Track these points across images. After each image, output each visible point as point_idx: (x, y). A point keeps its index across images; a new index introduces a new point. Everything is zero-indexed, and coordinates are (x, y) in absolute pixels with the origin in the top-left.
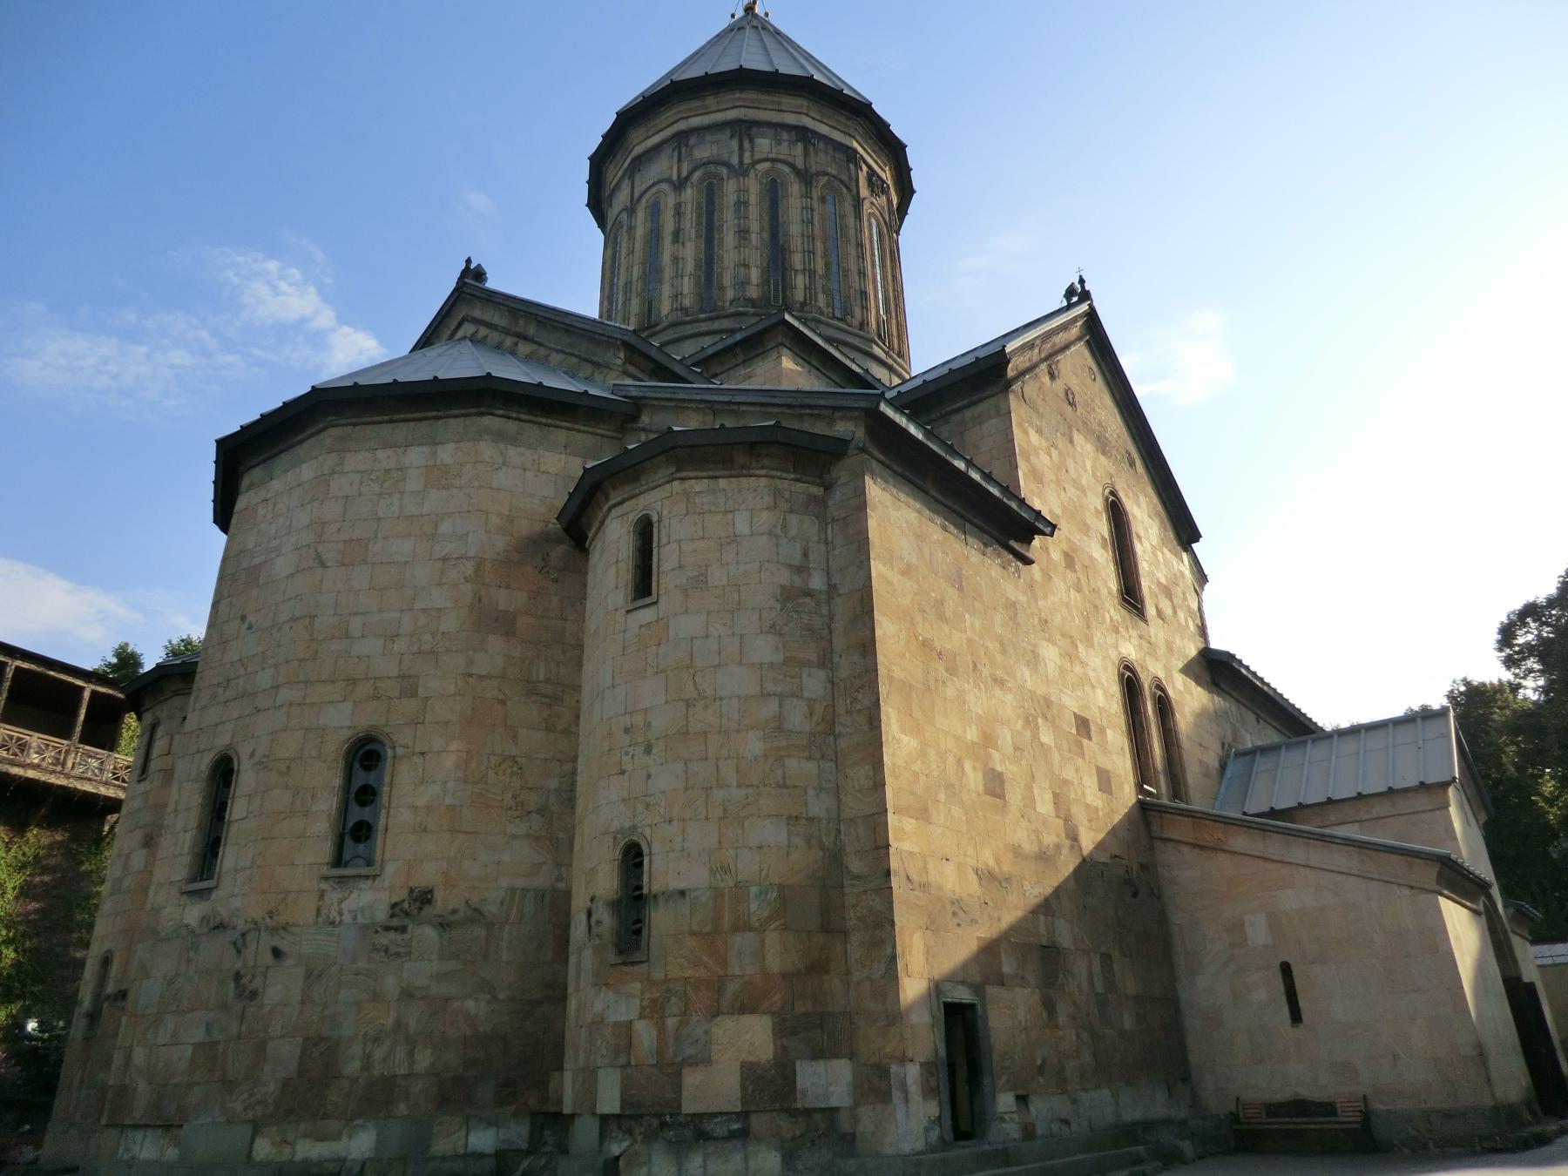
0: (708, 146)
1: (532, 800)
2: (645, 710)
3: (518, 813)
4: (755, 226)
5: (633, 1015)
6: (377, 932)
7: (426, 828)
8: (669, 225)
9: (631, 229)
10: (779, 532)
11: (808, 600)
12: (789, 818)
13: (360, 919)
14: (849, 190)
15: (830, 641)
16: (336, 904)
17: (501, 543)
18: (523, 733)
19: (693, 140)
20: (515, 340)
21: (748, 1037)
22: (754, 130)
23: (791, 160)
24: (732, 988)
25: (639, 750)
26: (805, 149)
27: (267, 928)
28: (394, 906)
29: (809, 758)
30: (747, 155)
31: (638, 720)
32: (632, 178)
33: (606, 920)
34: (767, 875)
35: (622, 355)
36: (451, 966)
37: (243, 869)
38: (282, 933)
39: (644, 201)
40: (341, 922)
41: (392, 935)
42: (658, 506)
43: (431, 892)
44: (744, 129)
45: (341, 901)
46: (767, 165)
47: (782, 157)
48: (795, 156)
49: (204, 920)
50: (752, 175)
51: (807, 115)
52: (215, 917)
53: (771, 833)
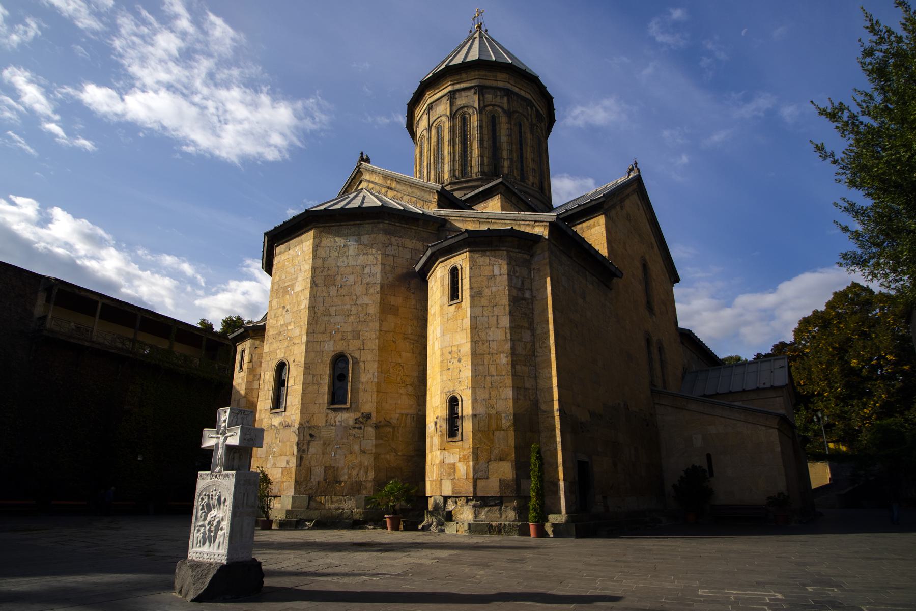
0: (463, 98)
1: (408, 380)
2: (458, 345)
3: (403, 385)
4: (486, 137)
5: (457, 459)
6: (350, 429)
7: (367, 390)
10: (512, 274)
11: (524, 302)
12: (517, 388)
13: (343, 424)
14: (528, 120)
15: (533, 319)
16: (333, 419)
17: (391, 277)
18: (404, 354)
20: (386, 190)
21: (502, 470)
22: (484, 90)
23: (501, 105)
24: (496, 451)
25: (456, 361)
26: (508, 100)
27: (307, 427)
28: (356, 419)
29: (525, 365)
30: (481, 103)
31: (455, 349)
32: (429, 114)
33: (444, 426)
34: (509, 410)
35: (436, 197)
36: (381, 442)
37: (294, 405)
38: (313, 429)
40: (335, 425)
41: (356, 430)
42: (461, 263)
43: (371, 414)
45: (335, 418)
46: (491, 108)
47: (497, 104)
48: (503, 103)
49: (281, 424)
50: (484, 113)
51: (508, 82)
52: (285, 422)
53: (509, 393)
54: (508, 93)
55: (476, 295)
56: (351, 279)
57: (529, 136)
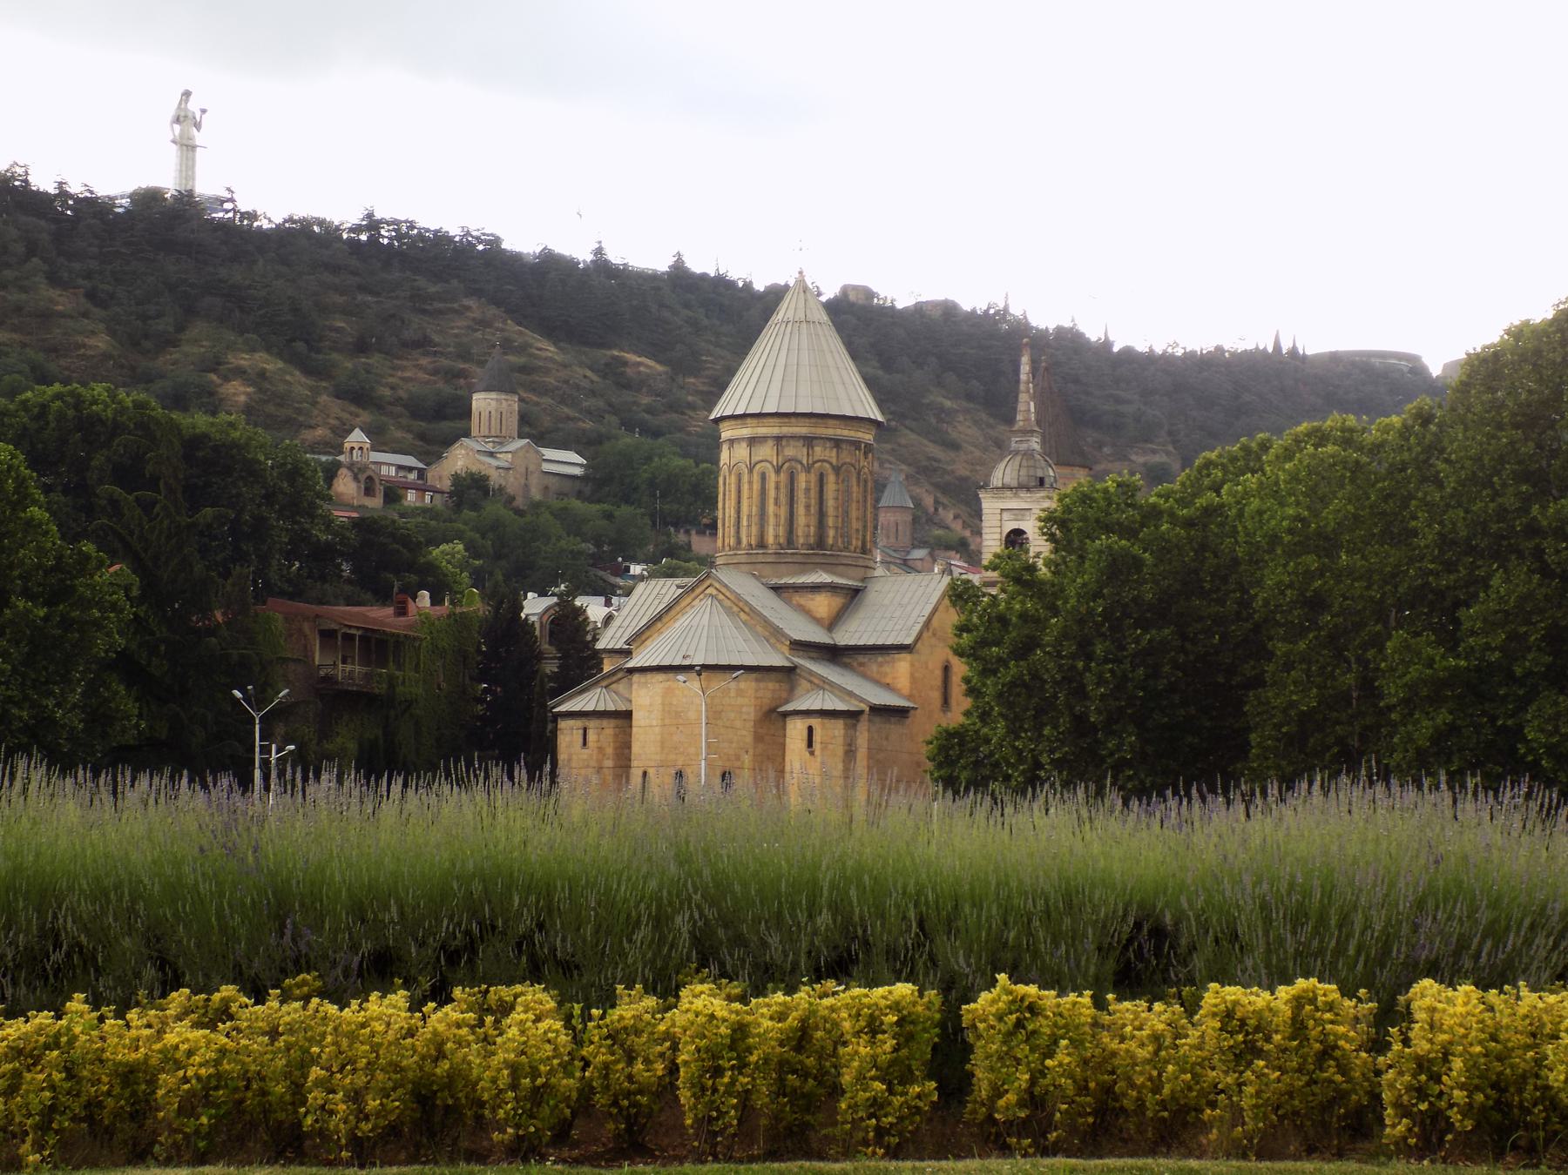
4: (813, 502)
8: (772, 493)
9: (750, 483)
19: (784, 443)
39: (758, 466)
44: (809, 441)
54: (837, 443)
55: (824, 749)
56: (732, 715)
57: (855, 489)
